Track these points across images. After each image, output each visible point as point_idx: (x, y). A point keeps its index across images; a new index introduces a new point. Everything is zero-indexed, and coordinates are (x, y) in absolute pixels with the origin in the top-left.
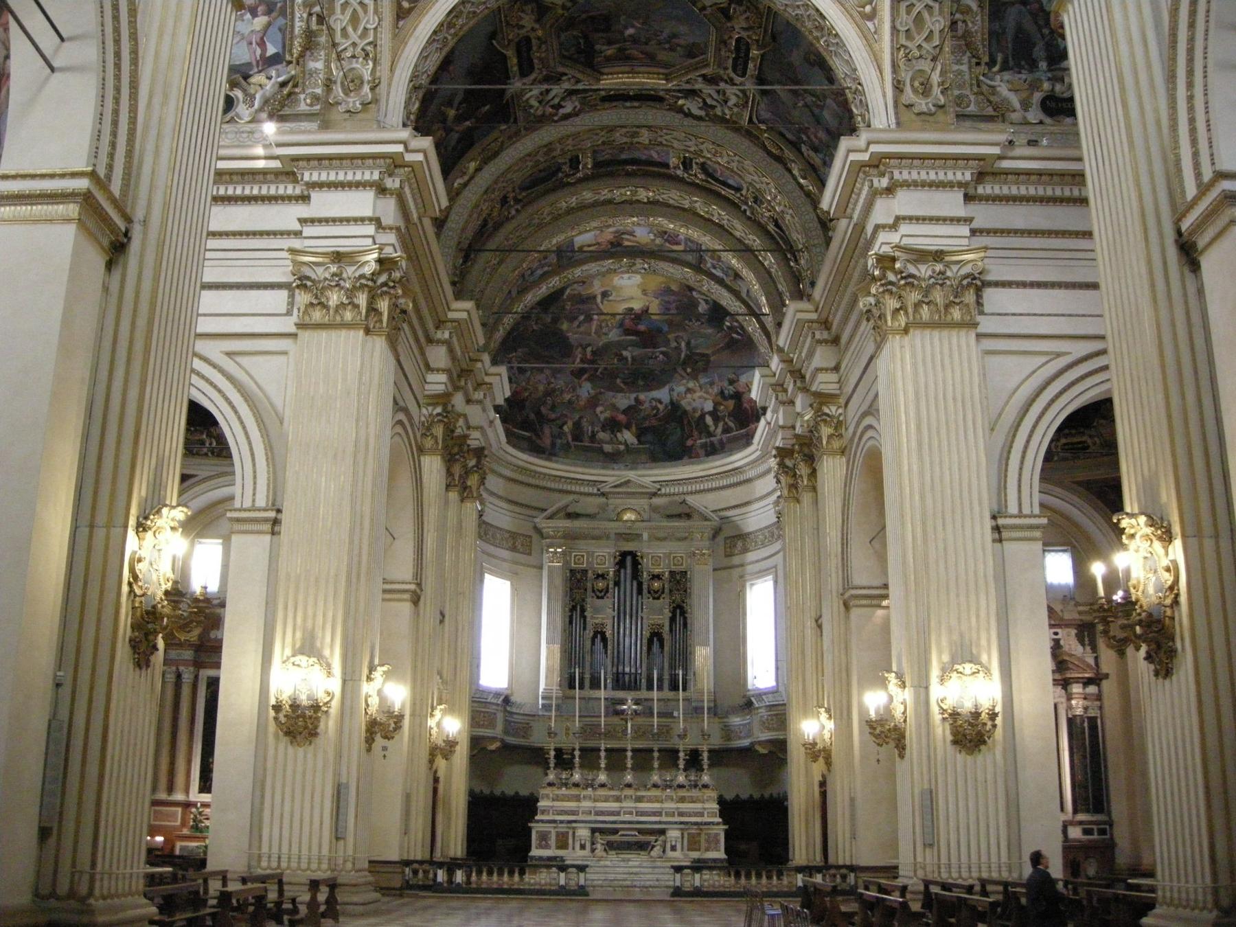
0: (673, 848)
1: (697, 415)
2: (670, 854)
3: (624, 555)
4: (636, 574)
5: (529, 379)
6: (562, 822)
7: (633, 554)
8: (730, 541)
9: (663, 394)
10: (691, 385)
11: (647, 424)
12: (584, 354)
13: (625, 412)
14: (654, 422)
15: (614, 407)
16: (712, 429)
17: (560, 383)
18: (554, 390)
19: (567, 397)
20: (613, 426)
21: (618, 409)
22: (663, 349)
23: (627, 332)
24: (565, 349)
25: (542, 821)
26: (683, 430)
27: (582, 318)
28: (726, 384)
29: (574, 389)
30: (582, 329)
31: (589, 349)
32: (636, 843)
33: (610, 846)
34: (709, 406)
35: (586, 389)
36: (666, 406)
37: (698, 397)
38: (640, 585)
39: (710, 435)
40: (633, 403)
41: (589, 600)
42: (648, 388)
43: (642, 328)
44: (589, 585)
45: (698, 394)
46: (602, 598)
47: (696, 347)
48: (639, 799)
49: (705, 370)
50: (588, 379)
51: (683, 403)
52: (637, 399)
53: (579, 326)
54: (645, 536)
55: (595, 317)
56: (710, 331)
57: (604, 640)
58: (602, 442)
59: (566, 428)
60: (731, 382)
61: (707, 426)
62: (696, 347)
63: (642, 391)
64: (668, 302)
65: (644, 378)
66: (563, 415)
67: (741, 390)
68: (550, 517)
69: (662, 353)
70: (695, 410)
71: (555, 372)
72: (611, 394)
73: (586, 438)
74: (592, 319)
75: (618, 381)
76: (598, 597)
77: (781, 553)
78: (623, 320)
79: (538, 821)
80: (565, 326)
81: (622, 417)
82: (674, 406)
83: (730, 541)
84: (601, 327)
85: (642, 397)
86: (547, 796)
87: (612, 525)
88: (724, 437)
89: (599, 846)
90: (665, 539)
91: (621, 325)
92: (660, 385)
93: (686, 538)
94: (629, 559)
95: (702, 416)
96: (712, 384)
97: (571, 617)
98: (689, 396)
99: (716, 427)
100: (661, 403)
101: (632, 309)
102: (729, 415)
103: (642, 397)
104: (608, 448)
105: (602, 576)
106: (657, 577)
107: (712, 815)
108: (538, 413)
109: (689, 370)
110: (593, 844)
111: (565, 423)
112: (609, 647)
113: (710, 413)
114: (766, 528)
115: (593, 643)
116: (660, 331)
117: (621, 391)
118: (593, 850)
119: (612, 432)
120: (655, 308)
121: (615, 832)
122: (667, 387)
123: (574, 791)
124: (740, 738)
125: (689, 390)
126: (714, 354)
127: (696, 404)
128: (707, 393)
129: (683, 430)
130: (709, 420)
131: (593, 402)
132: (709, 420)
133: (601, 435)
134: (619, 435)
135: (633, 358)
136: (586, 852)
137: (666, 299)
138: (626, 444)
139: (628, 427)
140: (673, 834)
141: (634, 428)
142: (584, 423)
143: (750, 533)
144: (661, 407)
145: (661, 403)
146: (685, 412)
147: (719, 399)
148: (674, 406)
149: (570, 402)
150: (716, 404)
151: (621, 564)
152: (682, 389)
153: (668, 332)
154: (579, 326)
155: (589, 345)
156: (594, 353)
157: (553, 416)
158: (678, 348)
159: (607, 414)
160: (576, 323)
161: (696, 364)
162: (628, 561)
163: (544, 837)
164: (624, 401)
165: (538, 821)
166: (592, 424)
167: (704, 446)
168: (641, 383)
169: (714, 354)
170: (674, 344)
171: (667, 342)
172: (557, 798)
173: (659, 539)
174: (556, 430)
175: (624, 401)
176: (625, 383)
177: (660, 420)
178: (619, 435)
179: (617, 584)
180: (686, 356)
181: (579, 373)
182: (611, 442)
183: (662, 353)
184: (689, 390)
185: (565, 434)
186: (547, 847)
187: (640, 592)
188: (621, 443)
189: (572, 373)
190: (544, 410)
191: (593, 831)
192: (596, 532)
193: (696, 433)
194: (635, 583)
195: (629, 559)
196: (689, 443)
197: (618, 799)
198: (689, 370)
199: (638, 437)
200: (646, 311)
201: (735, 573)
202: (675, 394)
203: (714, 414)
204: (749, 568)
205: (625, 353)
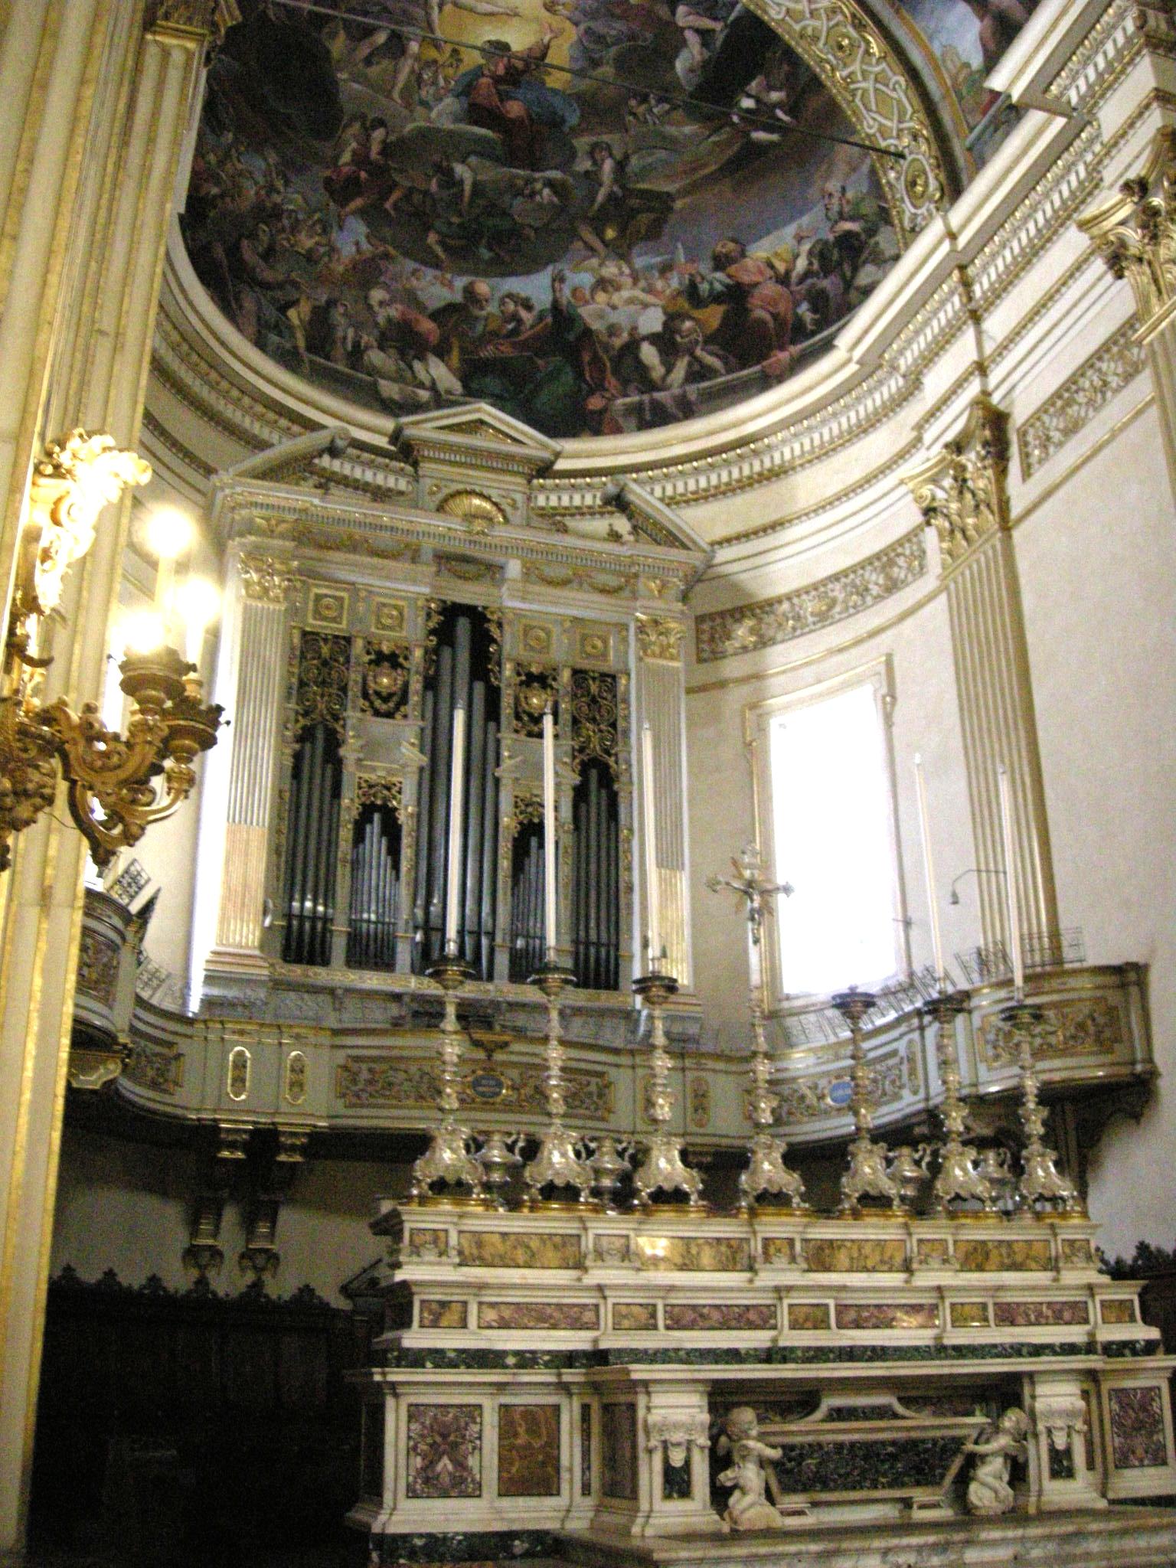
0: (1061, 1465)
1: (618, 342)
2: (1059, 1493)
3: (452, 612)
4: (482, 664)
5: (227, 156)
6: (527, 1360)
7: (477, 616)
8: (725, 621)
9: (536, 288)
10: (610, 270)
11: (488, 352)
12: (365, 142)
13: (435, 316)
14: (507, 350)
15: (411, 298)
16: (658, 371)
17: (293, 199)
18: (277, 213)
19: (306, 242)
20: (406, 341)
21: (420, 306)
22: (555, 174)
23: (477, 113)
24: (324, 111)
25: (439, 1358)
26: (579, 375)
27: (381, 38)
28: (704, 267)
29: (325, 231)
30: (374, 71)
31: (378, 134)
32: (909, 1447)
33: (793, 1473)
34: (652, 321)
35: (352, 239)
36: (541, 317)
37: (626, 299)
38: (493, 697)
39: (650, 386)
40: (458, 298)
41: (352, 715)
42: (502, 267)
43: (514, 109)
44: (354, 677)
45: (625, 294)
46: (389, 715)
47: (645, 172)
48: (821, 1257)
49: (653, 233)
50: (362, 213)
51: (585, 312)
52: (469, 292)
53: (368, 61)
54: (514, 568)
55: (414, 47)
56: (687, 129)
57: (392, 831)
58: (373, 371)
59: (292, 313)
60: (721, 262)
61: (642, 369)
62: (645, 172)
63: (486, 274)
64: (600, 39)
65: (497, 239)
66: (296, 285)
67: (746, 279)
68: (271, 473)
69: (549, 183)
70: (613, 330)
71: (289, 168)
72: (410, 265)
73: (339, 352)
74: (403, 51)
75: (432, 238)
76: (377, 713)
77: (943, 597)
78: (478, 72)
79: (416, 1359)
80: (338, 46)
81: (427, 326)
82: (562, 317)
83: (725, 621)
84: (419, 79)
85: (483, 287)
86: (437, 1241)
87: (439, 524)
88: (693, 391)
89: (750, 1475)
90: (565, 583)
91: (467, 89)
92: (531, 265)
93: (620, 588)
94: (463, 626)
95: (632, 346)
96: (665, 269)
97: (298, 757)
98: (601, 297)
99: (669, 371)
100: (529, 307)
101: (502, 47)
102: (709, 340)
103: (483, 287)
104: (390, 389)
105: (392, 660)
106: (541, 680)
107: (1118, 1311)
108: (233, 251)
109: (610, 234)
110: (720, 1461)
111: (294, 303)
112: (407, 853)
113: (654, 339)
114: (835, 578)
115: (359, 837)
116: (556, 122)
117: (437, 265)
118: (720, 1496)
119: (402, 354)
120: (561, 53)
121: (801, 1399)
122: (550, 268)
123: (554, 1221)
124: (813, 1113)
125: (602, 284)
126: (685, 192)
127: (619, 318)
128: (650, 290)
129: (579, 375)
130: (649, 354)
131: (366, 273)
132: (649, 354)
133: (376, 357)
134: (417, 365)
135: (475, 184)
136: (693, 1511)
137: (599, 27)
138: (433, 387)
139: (442, 353)
140: (1057, 1398)
141: (455, 357)
142: (338, 316)
143: (770, 604)
144: (524, 314)
145: (529, 307)
146: (587, 332)
147: (684, 304)
148: (562, 317)
149: (310, 257)
150: (672, 319)
151: (444, 634)
152: (586, 279)
153: (576, 131)
154: (368, 61)
155: (380, 123)
156: (386, 149)
157: (268, 275)
158: (591, 178)
159: (394, 312)
160: (364, 50)
161: (634, 218)
162: (465, 634)
163: (445, 1436)
164: (438, 289)
165: (416, 1359)
166: (358, 326)
167: (637, 410)
168: (485, 254)
169: (685, 192)
170: (584, 165)
171: (565, 165)
172: (476, 1253)
173: (550, 582)
174: (271, 314)
175: (438, 289)
176: (446, 248)
177: (524, 345)
178: (417, 365)
179: (431, 684)
180: (611, 197)
181: (342, 190)
182: (398, 378)
183: (549, 183)
184: (602, 284)
185: (291, 328)
186: (463, 1486)
187: (492, 713)
188: (421, 385)
189: (328, 182)
190: (249, 253)
191: (723, 1398)
192: (384, 539)
193: (612, 382)
194: (479, 688)
195: (463, 626)
196: (595, 403)
197: (733, 1256)
198: (610, 234)
199: (465, 380)
200: (537, 58)
201: (735, 697)
202: (567, 292)
203: (667, 342)
204: (775, 683)
205: (460, 169)
